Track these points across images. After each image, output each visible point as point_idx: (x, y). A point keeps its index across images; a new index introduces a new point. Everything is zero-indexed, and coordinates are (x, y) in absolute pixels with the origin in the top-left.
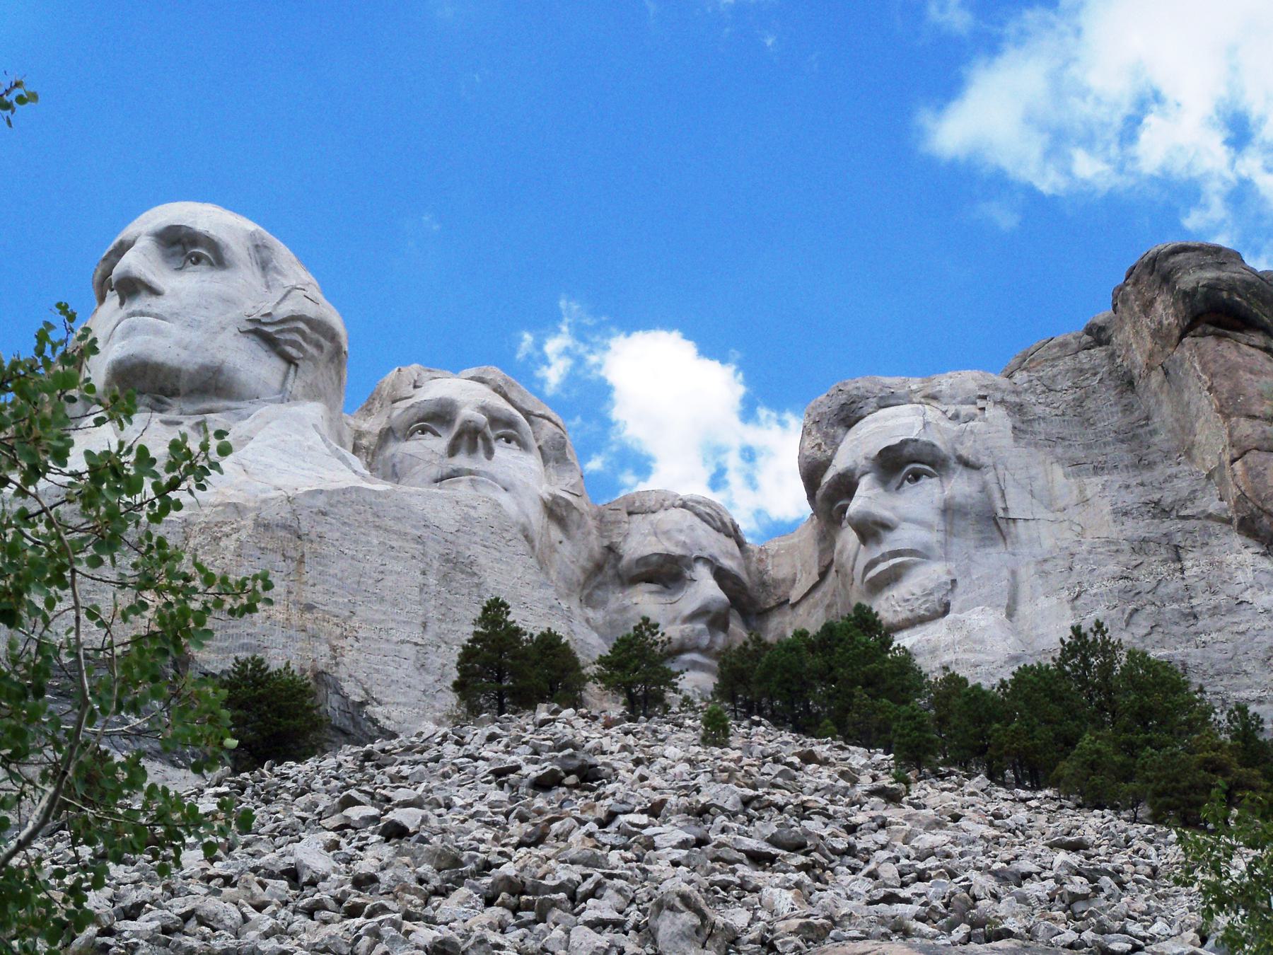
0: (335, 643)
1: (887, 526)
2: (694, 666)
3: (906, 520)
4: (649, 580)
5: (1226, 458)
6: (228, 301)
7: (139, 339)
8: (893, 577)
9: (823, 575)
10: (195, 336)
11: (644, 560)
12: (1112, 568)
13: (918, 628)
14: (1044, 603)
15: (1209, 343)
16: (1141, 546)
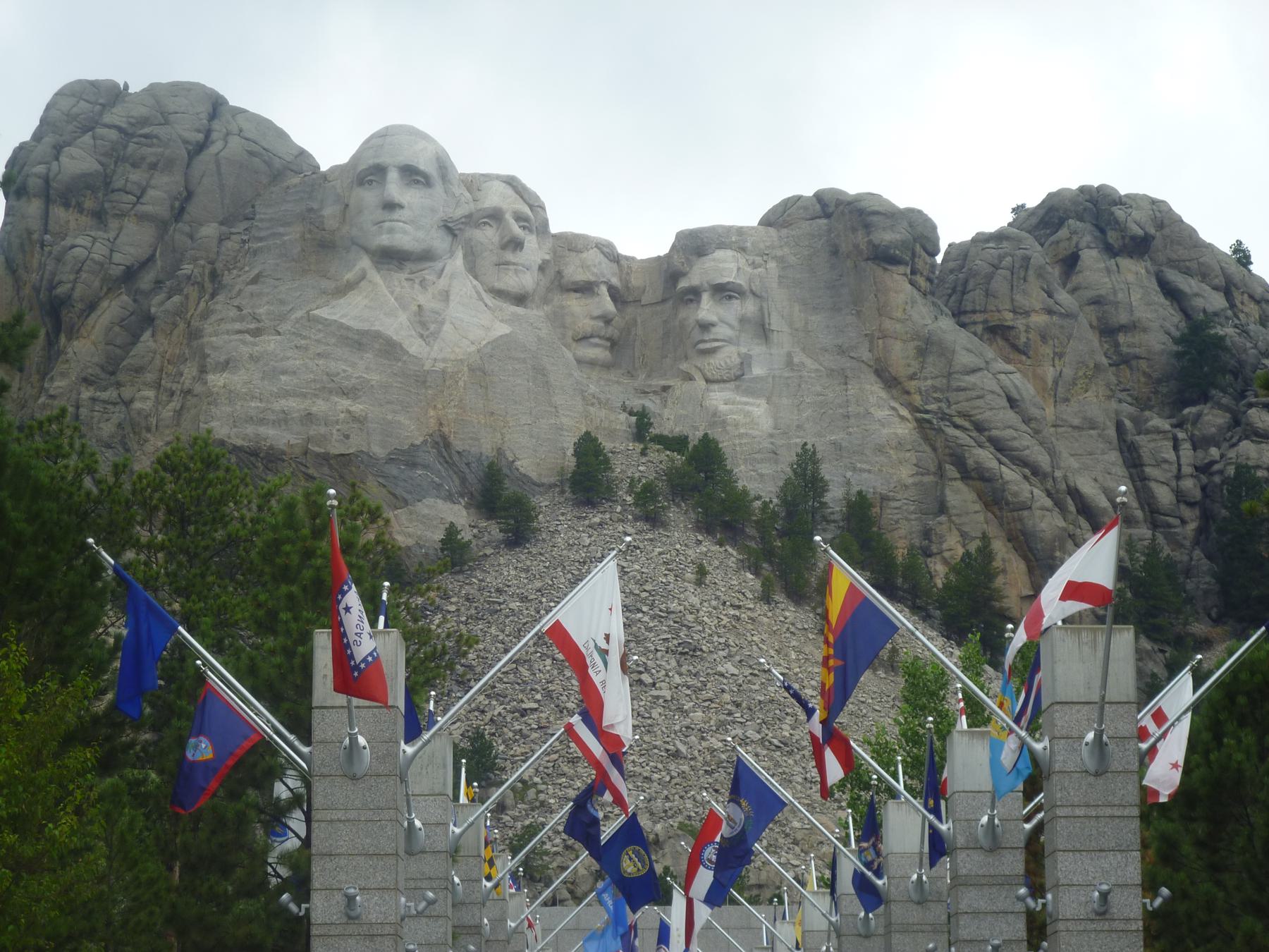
0: (504, 431)
1: (713, 325)
2: (596, 345)
3: (722, 321)
4: (576, 291)
5: (877, 334)
6: (433, 210)
7: (398, 236)
8: (712, 352)
9: (664, 301)
10: (421, 234)
11: (574, 283)
12: (819, 389)
13: (722, 385)
14: (785, 401)
15: (879, 271)
16: (831, 373)
